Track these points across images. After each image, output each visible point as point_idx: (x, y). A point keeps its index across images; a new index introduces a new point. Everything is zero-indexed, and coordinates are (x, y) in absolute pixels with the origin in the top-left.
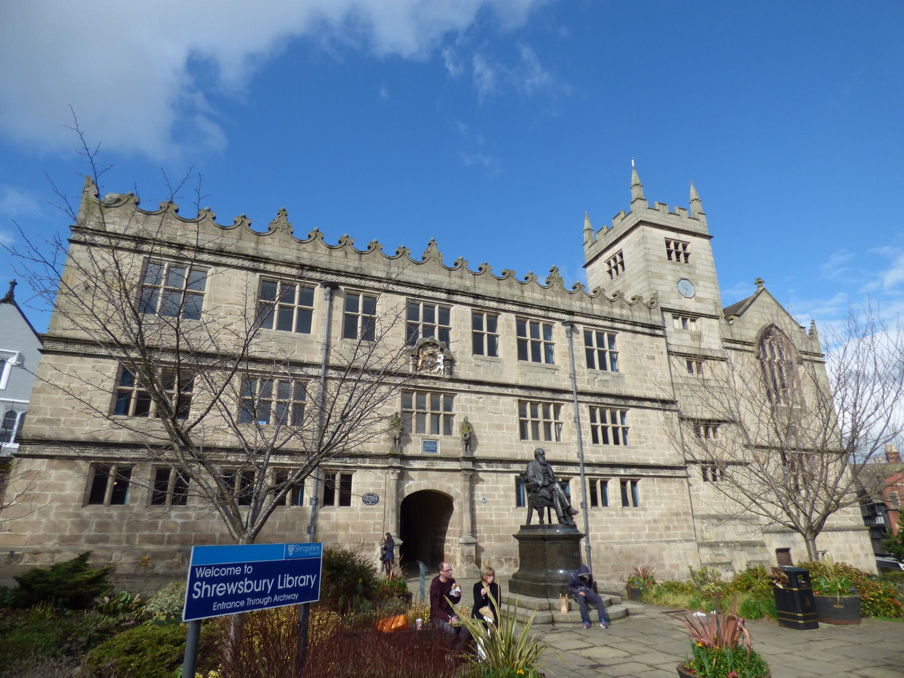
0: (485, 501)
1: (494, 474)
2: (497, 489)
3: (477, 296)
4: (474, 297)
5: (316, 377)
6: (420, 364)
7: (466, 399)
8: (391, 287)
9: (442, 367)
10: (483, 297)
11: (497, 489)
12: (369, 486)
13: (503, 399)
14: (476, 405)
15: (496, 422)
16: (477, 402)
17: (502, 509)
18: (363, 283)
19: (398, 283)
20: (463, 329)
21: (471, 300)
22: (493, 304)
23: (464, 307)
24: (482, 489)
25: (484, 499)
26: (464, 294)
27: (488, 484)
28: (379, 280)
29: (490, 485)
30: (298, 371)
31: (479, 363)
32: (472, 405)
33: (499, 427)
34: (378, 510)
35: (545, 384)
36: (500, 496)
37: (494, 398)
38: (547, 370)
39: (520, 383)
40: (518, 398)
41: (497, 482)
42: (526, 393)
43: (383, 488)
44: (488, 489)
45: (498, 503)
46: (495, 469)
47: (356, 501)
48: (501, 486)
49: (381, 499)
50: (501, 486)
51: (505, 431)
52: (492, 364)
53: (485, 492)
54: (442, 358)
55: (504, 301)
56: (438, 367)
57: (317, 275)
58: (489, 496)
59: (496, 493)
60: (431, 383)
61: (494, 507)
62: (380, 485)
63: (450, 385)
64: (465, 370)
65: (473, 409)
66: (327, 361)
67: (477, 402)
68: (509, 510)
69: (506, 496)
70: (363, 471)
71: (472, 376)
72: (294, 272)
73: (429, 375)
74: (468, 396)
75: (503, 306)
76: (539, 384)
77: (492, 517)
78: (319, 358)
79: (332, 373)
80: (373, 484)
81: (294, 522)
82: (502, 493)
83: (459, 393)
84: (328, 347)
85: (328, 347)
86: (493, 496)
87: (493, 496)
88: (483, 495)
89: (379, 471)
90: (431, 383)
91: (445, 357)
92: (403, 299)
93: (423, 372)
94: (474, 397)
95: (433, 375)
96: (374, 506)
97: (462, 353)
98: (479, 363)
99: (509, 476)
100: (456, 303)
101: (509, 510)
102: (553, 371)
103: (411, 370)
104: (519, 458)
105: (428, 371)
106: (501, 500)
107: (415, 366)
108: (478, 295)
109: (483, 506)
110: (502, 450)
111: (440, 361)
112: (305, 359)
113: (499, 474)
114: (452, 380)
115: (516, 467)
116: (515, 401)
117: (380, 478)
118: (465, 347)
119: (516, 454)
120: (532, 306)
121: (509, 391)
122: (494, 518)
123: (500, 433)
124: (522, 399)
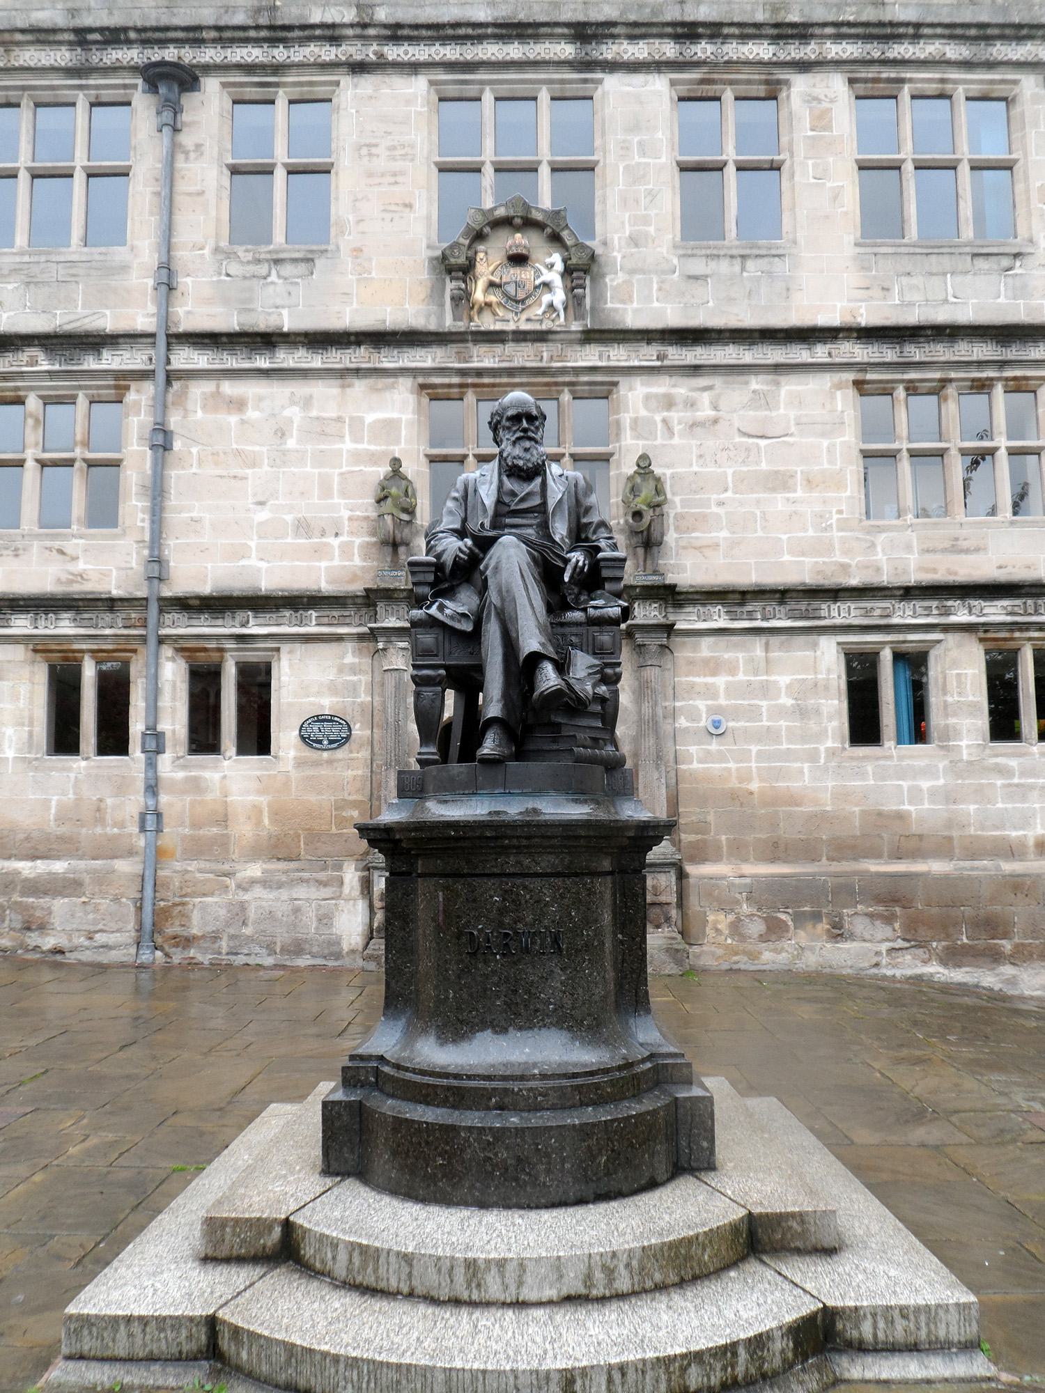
0: (716, 731)
1: (758, 643)
2: (766, 690)
3: (688, 32)
4: (677, 38)
5: (144, 375)
6: (479, 295)
7: (647, 398)
8: (369, 52)
9: (558, 296)
10: (715, 31)
11: (766, 690)
12: (319, 694)
13: (791, 386)
14: (688, 415)
15: (764, 466)
16: (691, 404)
17: (788, 755)
18: (280, 54)
19: (396, 33)
20: (637, 159)
21: (669, 50)
22: (762, 50)
23: (638, 79)
24: (710, 692)
25: (717, 724)
26: (638, 30)
27: (733, 671)
28: (331, 34)
29: (741, 677)
30: (90, 363)
31: (698, 267)
32: (674, 416)
33: (779, 481)
34: (349, 763)
35: (966, 315)
36: (781, 712)
37: (756, 383)
38: (981, 263)
39: (864, 320)
40: (850, 376)
41: (769, 665)
42: (889, 354)
43: (364, 698)
44: (731, 690)
45: (770, 735)
46: (758, 624)
47: (284, 735)
48: (784, 680)
49: (360, 731)
50: (784, 680)
51: (799, 494)
52: (750, 264)
53: (722, 701)
54: (559, 266)
55: (801, 32)
56: (546, 298)
57: (132, 55)
58: (736, 713)
59: (764, 703)
60: (523, 356)
61: (754, 749)
62: (354, 689)
63: (590, 356)
64: (648, 299)
65: (677, 428)
66: (166, 317)
67: (691, 404)
68: (813, 757)
69: (802, 712)
70: (299, 648)
71: (674, 318)
72: (62, 56)
73: (511, 326)
74: (662, 386)
75: (794, 51)
76: (942, 316)
77: (750, 780)
78: (143, 319)
79: (186, 358)
80: (333, 689)
81: (101, 800)
82: (789, 702)
83: (624, 382)
84: (167, 284)
85: (167, 284)
86: (754, 713)
87: (754, 713)
88: (711, 710)
89: (349, 646)
90: (523, 356)
91: (565, 261)
92: (419, 85)
93: (487, 323)
94: (681, 388)
95: (525, 326)
96: (341, 754)
97: (634, 241)
98: (698, 267)
99: (815, 646)
100: (613, 66)
101: (813, 757)
102: (1005, 262)
103: (449, 323)
104: (854, 582)
105: (510, 316)
106: (783, 723)
107: (462, 300)
108: (694, 24)
109: (714, 746)
110: (786, 558)
111: (554, 277)
112: (108, 323)
113: (775, 640)
114: (592, 336)
115: (841, 613)
116: (839, 386)
117: (354, 670)
118: (646, 220)
119: (845, 567)
120: (916, 31)
121: (820, 353)
122: (754, 786)
123: (779, 503)
124: (869, 376)
